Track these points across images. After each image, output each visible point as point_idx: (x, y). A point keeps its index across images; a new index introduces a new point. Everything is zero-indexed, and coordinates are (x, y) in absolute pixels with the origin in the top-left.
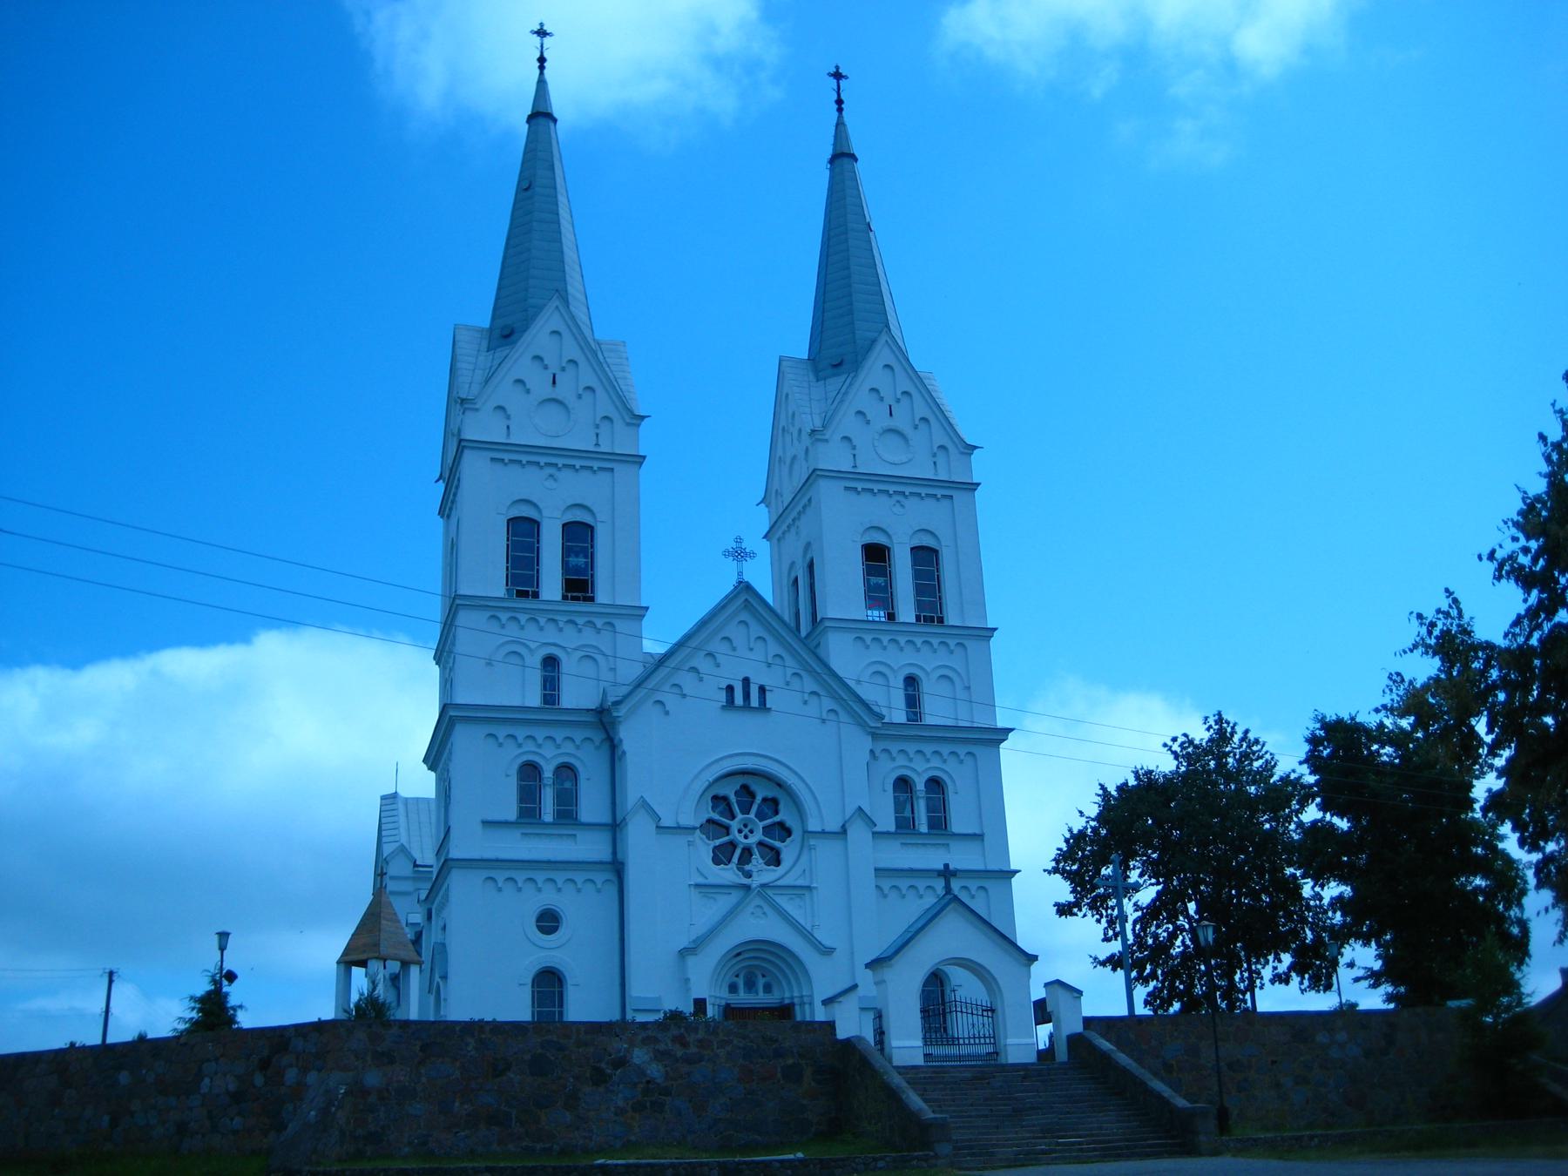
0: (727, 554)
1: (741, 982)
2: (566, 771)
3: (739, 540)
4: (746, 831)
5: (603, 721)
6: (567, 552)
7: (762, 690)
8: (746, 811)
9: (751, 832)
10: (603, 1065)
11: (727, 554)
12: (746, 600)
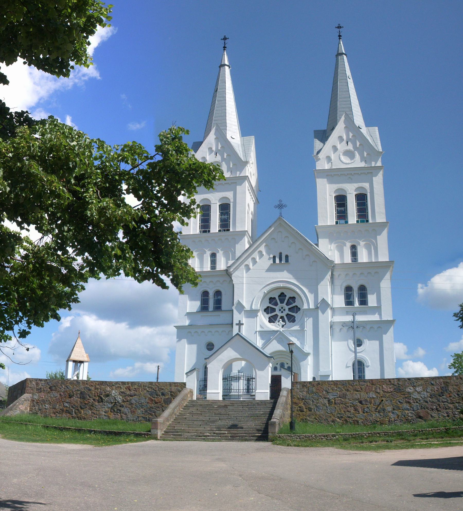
0: (276, 207)
1: (278, 366)
2: (218, 293)
3: (280, 201)
4: (282, 310)
5: (227, 273)
6: (221, 214)
7: (287, 257)
8: (282, 302)
9: (284, 310)
10: (102, 396)
11: (276, 207)
12: (280, 223)
